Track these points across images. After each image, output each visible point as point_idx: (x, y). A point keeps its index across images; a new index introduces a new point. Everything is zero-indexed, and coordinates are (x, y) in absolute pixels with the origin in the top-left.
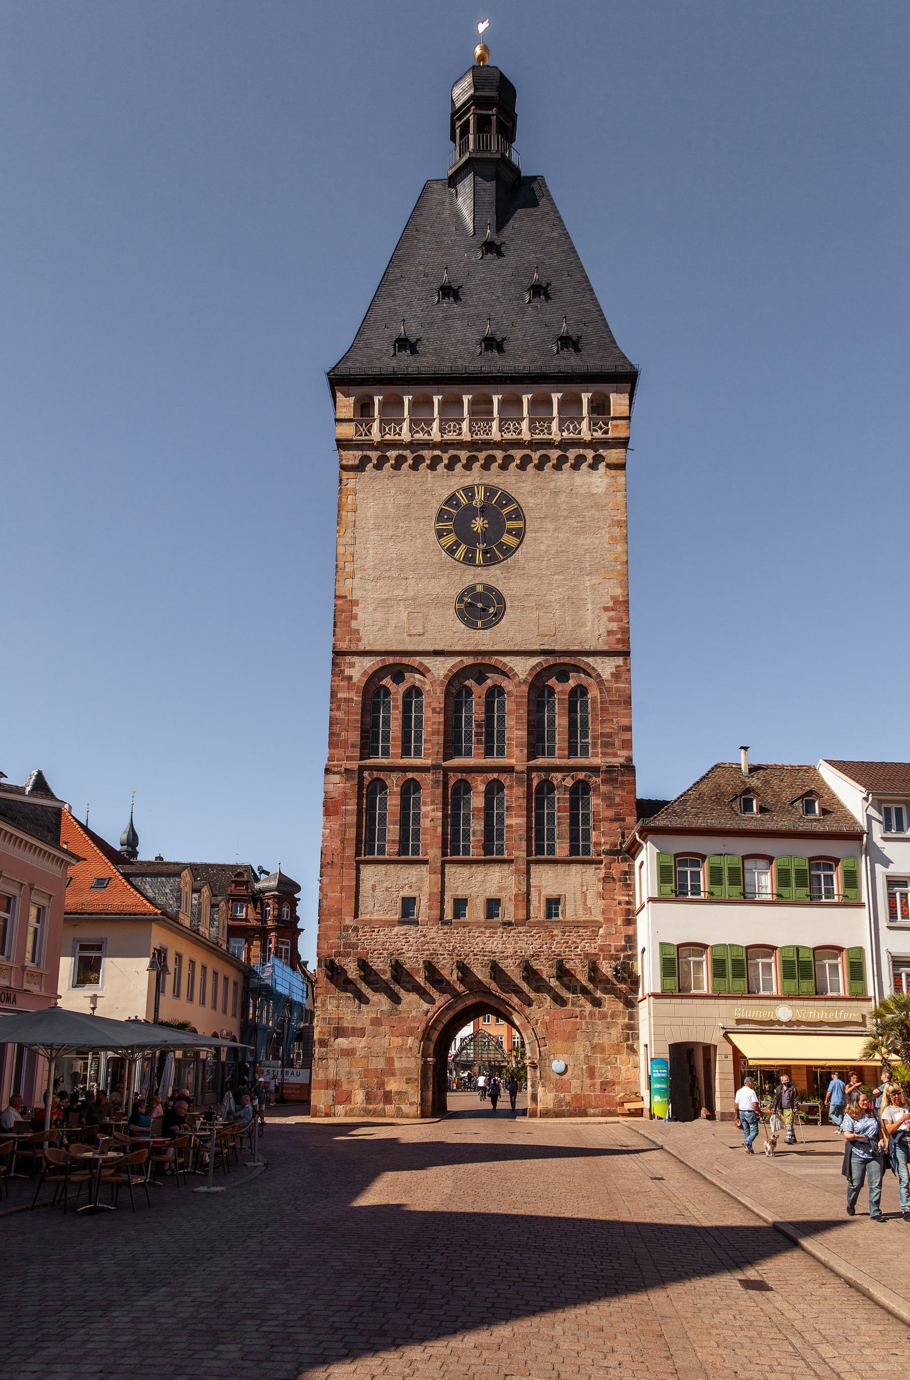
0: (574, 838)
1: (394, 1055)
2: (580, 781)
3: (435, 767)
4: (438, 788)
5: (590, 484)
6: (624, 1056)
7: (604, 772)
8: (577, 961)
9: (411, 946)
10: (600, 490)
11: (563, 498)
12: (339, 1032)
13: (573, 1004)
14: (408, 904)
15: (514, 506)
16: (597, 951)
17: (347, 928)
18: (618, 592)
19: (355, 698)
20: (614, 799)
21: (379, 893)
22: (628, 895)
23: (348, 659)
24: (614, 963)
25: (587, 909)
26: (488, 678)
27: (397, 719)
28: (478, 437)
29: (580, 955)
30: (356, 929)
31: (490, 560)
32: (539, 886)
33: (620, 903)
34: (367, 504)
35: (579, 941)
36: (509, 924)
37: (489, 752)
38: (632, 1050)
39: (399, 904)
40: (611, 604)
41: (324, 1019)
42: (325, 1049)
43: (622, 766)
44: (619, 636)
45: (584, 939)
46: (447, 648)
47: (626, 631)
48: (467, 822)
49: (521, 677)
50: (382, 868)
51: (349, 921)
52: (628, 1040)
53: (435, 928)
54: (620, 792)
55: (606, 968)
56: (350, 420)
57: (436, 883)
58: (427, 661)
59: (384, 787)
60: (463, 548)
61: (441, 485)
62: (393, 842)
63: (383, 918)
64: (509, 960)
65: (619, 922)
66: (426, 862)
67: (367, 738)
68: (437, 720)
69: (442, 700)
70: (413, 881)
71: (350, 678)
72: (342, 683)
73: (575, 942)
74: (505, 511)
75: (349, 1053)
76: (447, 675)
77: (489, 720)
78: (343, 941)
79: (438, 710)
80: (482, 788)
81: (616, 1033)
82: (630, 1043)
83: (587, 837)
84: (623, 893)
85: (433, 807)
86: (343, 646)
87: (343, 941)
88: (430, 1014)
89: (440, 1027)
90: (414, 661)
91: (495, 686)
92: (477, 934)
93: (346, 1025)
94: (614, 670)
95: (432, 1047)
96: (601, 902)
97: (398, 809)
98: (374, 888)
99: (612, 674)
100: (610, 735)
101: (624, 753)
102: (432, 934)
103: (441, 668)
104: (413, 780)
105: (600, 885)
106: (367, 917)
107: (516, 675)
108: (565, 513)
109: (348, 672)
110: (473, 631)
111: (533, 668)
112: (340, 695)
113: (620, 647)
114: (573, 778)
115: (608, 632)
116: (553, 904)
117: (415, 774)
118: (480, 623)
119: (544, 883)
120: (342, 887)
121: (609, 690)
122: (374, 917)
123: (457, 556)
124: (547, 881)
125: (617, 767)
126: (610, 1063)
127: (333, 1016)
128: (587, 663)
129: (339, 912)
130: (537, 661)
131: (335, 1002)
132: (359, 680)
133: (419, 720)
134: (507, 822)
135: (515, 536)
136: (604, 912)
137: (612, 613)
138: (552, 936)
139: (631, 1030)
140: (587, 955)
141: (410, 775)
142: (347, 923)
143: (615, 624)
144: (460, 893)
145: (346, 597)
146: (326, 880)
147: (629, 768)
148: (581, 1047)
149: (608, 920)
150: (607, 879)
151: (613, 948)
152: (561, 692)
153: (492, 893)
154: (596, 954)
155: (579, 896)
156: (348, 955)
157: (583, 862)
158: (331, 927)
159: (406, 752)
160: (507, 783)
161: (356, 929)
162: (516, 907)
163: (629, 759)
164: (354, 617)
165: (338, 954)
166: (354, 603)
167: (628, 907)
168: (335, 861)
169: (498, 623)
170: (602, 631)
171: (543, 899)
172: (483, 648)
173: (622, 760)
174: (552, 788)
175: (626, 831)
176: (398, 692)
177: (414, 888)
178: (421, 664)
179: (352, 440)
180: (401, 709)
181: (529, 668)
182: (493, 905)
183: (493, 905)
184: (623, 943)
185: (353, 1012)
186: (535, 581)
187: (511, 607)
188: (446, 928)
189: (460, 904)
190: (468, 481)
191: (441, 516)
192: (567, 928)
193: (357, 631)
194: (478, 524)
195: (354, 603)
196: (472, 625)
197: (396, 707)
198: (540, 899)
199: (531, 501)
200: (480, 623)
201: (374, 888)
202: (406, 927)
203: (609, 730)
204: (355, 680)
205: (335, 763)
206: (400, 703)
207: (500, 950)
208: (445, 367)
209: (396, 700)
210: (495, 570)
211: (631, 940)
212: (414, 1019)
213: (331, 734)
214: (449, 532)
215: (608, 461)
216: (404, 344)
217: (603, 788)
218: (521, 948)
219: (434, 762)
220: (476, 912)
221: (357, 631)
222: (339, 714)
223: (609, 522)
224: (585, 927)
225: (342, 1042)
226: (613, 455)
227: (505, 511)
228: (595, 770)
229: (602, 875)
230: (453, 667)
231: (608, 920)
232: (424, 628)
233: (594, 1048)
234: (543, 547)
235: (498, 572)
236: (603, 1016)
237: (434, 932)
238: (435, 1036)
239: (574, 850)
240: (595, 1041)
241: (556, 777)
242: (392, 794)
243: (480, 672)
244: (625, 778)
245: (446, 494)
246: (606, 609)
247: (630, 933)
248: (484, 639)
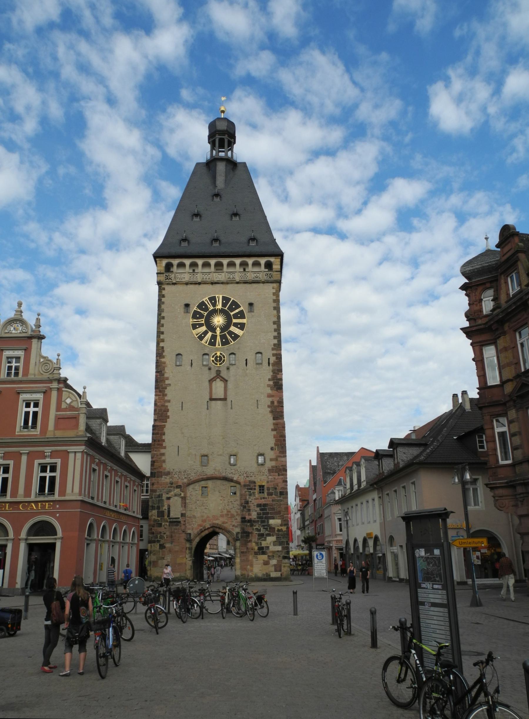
56: (163, 273)
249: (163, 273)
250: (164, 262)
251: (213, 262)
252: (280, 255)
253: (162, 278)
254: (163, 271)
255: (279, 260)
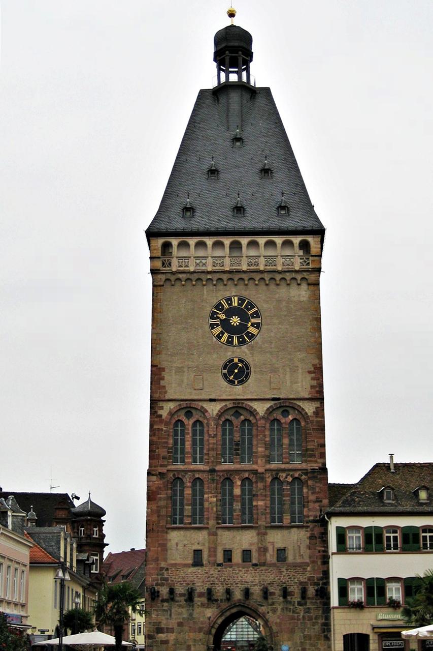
0: (293, 513)
1: (191, 643)
2: (296, 478)
3: (212, 471)
4: (213, 483)
5: (300, 295)
6: (323, 642)
7: (310, 472)
8: (295, 587)
9: (199, 579)
10: (305, 299)
11: (284, 304)
12: (160, 630)
13: (294, 612)
14: (198, 553)
15: (255, 309)
16: (306, 580)
17: (162, 569)
18: (317, 361)
19: (164, 429)
20: (315, 489)
21: (180, 547)
22: (324, 547)
23: (161, 404)
24: (316, 588)
25: (301, 556)
26: (242, 415)
27: (188, 441)
28: (234, 268)
29: (296, 583)
30: (167, 569)
31: (242, 342)
32: (273, 542)
33: (319, 552)
34: (168, 308)
35: (296, 575)
36: (256, 565)
37: (243, 460)
38: (327, 638)
39: (193, 553)
40: (312, 369)
41: (150, 623)
42: (151, 641)
43: (320, 468)
44: (317, 389)
45: (299, 574)
46: (217, 398)
47: (321, 386)
48: (231, 504)
49: (260, 414)
50: (182, 532)
51: (163, 564)
52: (324, 632)
53: (213, 568)
54: (318, 485)
55: (311, 591)
56: (159, 258)
57: (213, 541)
58: (206, 405)
59: (182, 483)
60: (226, 335)
61: (212, 296)
62: (188, 516)
63: (183, 562)
64: (256, 587)
65: (319, 563)
66: (208, 528)
67: (171, 452)
68: (213, 442)
69: (215, 429)
70: (201, 540)
71: (161, 416)
72: (156, 419)
73: (294, 575)
74: (250, 312)
75: (166, 642)
76: (217, 414)
77: (243, 440)
78: (159, 577)
79: (213, 435)
80: (239, 483)
81: (317, 628)
82: (326, 633)
83: (301, 512)
84: (321, 545)
85: (212, 495)
86: (156, 396)
87: (159, 577)
88: (211, 619)
89: (217, 626)
90: (198, 405)
91: (246, 420)
92: (237, 572)
93: (163, 626)
94: (315, 410)
95: (212, 639)
96: (308, 551)
97: (190, 497)
98: (177, 544)
99: (314, 412)
100: (313, 450)
101: (320, 461)
102: (212, 572)
103: (214, 409)
104: (198, 478)
105: (308, 541)
106: (173, 562)
107: (258, 413)
108: (286, 313)
109: (160, 412)
110: (233, 386)
111: (268, 409)
112: (155, 427)
113: (318, 396)
114: (292, 476)
115: (311, 386)
116: (281, 553)
117: (201, 474)
118: (236, 383)
119: (276, 540)
120: (159, 544)
121: (312, 422)
122: (177, 562)
123: (222, 340)
124: (277, 539)
125: (317, 469)
126: (315, 646)
127: (155, 621)
128: (299, 406)
129: (157, 560)
130: (269, 406)
131: (155, 612)
132: (166, 417)
133: (202, 441)
134: (254, 503)
135: (255, 327)
136: (310, 558)
137: (313, 375)
138: (281, 572)
139: (326, 628)
140: (301, 583)
141: (197, 476)
142: (162, 565)
143: (315, 381)
144: (228, 547)
145: (157, 366)
146: (149, 540)
147: (324, 470)
148: (298, 636)
149: (313, 562)
150: (312, 537)
151: (315, 578)
152: (285, 423)
153: (246, 546)
154: (305, 582)
155: (296, 546)
156: (162, 585)
157: (298, 527)
158: (153, 568)
159: (195, 461)
160: (254, 480)
161: (167, 569)
162: (259, 555)
163: (324, 464)
164: (163, 379)
165: (157, 584)
166: (163, 369)
167: (325, 554)
168: (154, 528)
169: (247, 381)
170: (308, 387)
171: (275, 550)
172: (238, 397)
173: (320, 465)
174: (281, 483)
175: (323, 508)
176: (189, 424)
177: (200, 544)
178: (202, 407)
179: (159, 270)
180: (191, 435)
181: (265, 409)
182: (246, 554)
183: (246, 554)
184: (321, 575)
185: (167, 619)
186: (268, 355)
187: (255, 371)
188: (219, 568)
189: (228, 555)
190: (228, 294)
191: (213, 316)
192: (290, 567)
193: (164, 387)
194: (235, 320)
195: (163, 369)
196: (232, 382)
197: (188, 434)
198: (273, 550)
199: (265, 306)
200: (236, 383)
201: (177, 544)
202: (196, 568)
203: (312, 447)
204: (164, 417)
205: (153, 468)
206: (190, 431)
207: (251, 580)
208: (213, 225)
209: (188, 429)
210: (244, 348)
211: (326, 574)
212: (202, 623)
213: (151, 451)
214: (217, 325)
215: (310, 282)
216: (188, 210)
217: (310, 483)
218: (263, 579)
219: (211, 468)
220: (237, 558)
221: (164, 387)
222: (155, 439)
223: (311, 318)
224: (299, 567)
225: (162, 636)
226: (311, 278)
227: (250, 312)
228: (305, 472)
229: (308, 535)
230: (221, 409)
231: (313, 562)
232: (203, 385)
233: (305, 637)
234: (272, 334)
235: (246, 350)
236: (310, 619)
237: (214, 571)
238: (214, 631)
239: (293, 520)
240: (306, 633)
241: (282, 475)
242: (188, 487)
243: (237, 411)
244: (322, 476)
245: (215, 302)
246: (310, 372)
247: (326, 569)
248: (238, 392)
249: (159, 258)
250: (160, 241)
251: (227, 241)
252: (320, 232)
253: (158, 264)
254: (159, 254)
255: (319, 239)
